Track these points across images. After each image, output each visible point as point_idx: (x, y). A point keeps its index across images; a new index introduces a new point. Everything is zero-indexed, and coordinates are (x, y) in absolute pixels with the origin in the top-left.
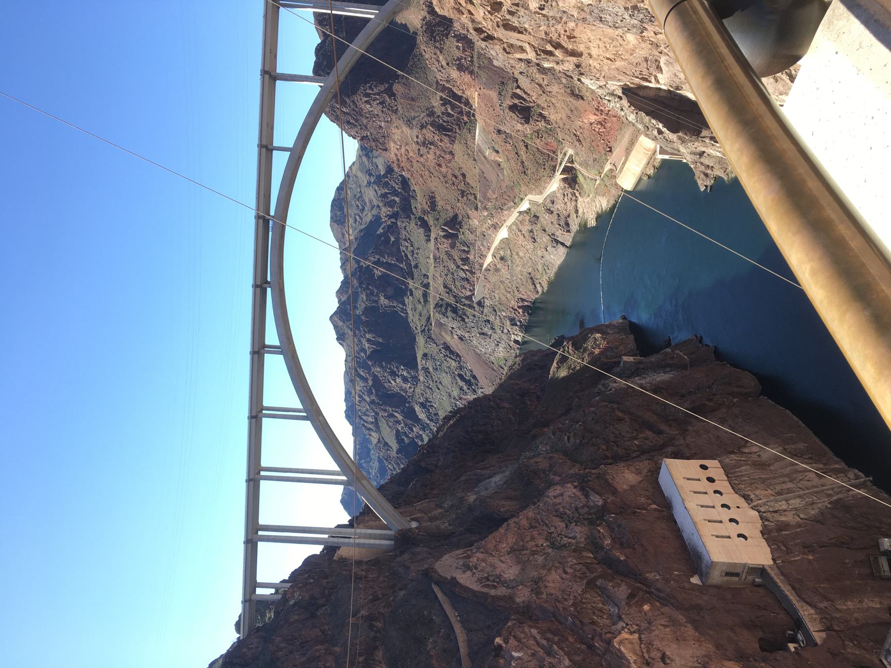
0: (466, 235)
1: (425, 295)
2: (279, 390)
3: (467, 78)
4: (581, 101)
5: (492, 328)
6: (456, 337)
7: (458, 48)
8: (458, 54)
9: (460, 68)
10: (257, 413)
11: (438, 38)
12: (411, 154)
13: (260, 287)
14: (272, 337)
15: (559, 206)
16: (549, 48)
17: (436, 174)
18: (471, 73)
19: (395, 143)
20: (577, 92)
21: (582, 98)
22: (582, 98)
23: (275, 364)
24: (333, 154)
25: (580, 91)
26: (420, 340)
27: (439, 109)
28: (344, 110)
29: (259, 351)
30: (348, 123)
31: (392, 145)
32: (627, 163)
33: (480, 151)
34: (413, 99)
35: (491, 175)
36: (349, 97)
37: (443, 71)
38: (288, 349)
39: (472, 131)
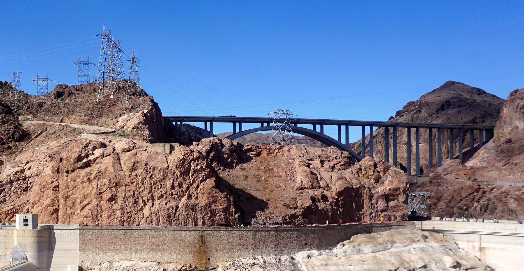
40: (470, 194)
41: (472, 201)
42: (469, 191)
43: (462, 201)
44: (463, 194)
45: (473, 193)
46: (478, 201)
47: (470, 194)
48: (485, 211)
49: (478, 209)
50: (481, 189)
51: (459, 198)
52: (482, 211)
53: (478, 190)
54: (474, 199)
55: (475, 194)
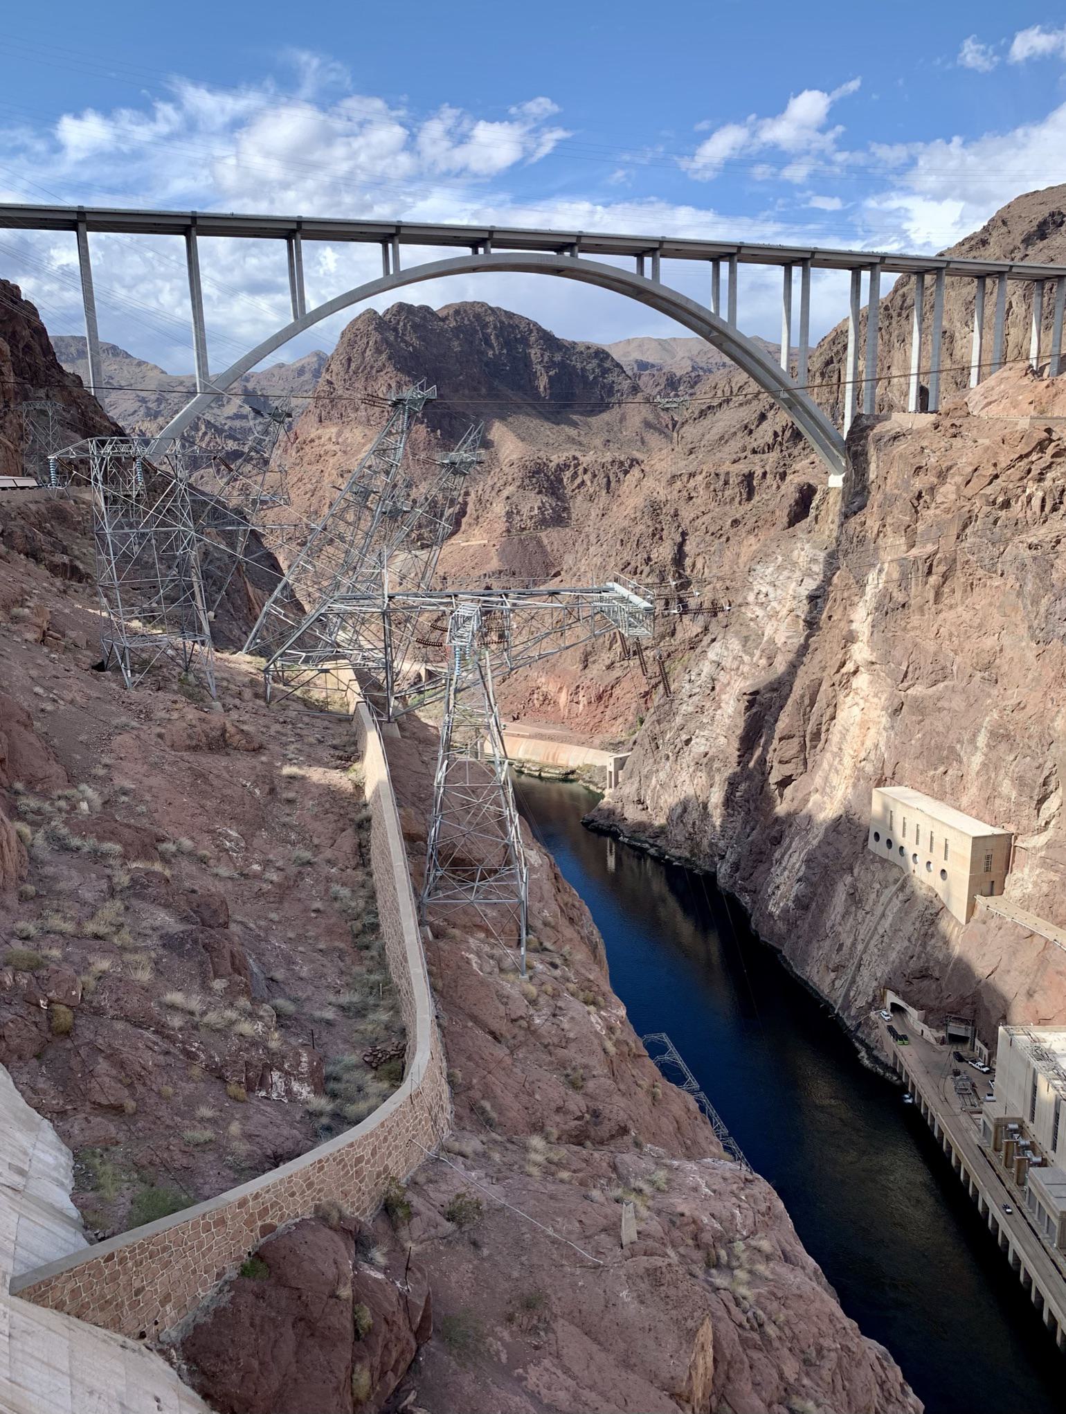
3: (501, 526)
4: (581, 667)
7: (532, 509)
8: (525, 511)
9: (509, 515)
11: (534, 480)
12: (331, 461)
13: (477, 239)
16: (939, 569)
17: (314, 500)
18: (508, 531)
19: (339, 434)
20: (591, 660)
21: (585, 667)
22: (585, 667)
25: (594, 662)
27: (414, 493)
28: (368, 353)
30: (349, 360)
31: (334, 430)
32: (524, 740)
36: (390, 359)
37: (494, 494)
40: (1021, 457)
41: (1021, 479)
42: (1023, 449)
43: (999, 481)
44: (1001, 459)
45: (1028, 455)
46: (1041, 478)
47: (1021, 457)
48: (1055, 509)
49: (1036, 503)
50: (1051, 441)
51: (991, 471)
52: (1047, 509)
53: (1041, 446)
54: (1029, 471)
55: (1034, 457)
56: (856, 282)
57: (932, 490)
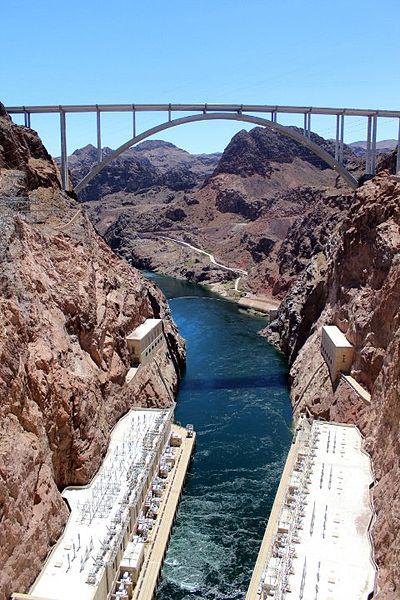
0: (176, 224)
1: (127, 203)
2: (147, 121)
5: (124, 246)
6: (108, 225)
10: (134, 108)
14: (176, 115)
15: (214, 272)
23: (162, 117)
24: (208, 140)
26: (96, 204)
29: (170, 108)
33: (232, 226)
34: (252, 186)
35: (218, 234)
38: (171, 124)
39: (241, 221)
56: (370, 119)
57: (359, 206)
